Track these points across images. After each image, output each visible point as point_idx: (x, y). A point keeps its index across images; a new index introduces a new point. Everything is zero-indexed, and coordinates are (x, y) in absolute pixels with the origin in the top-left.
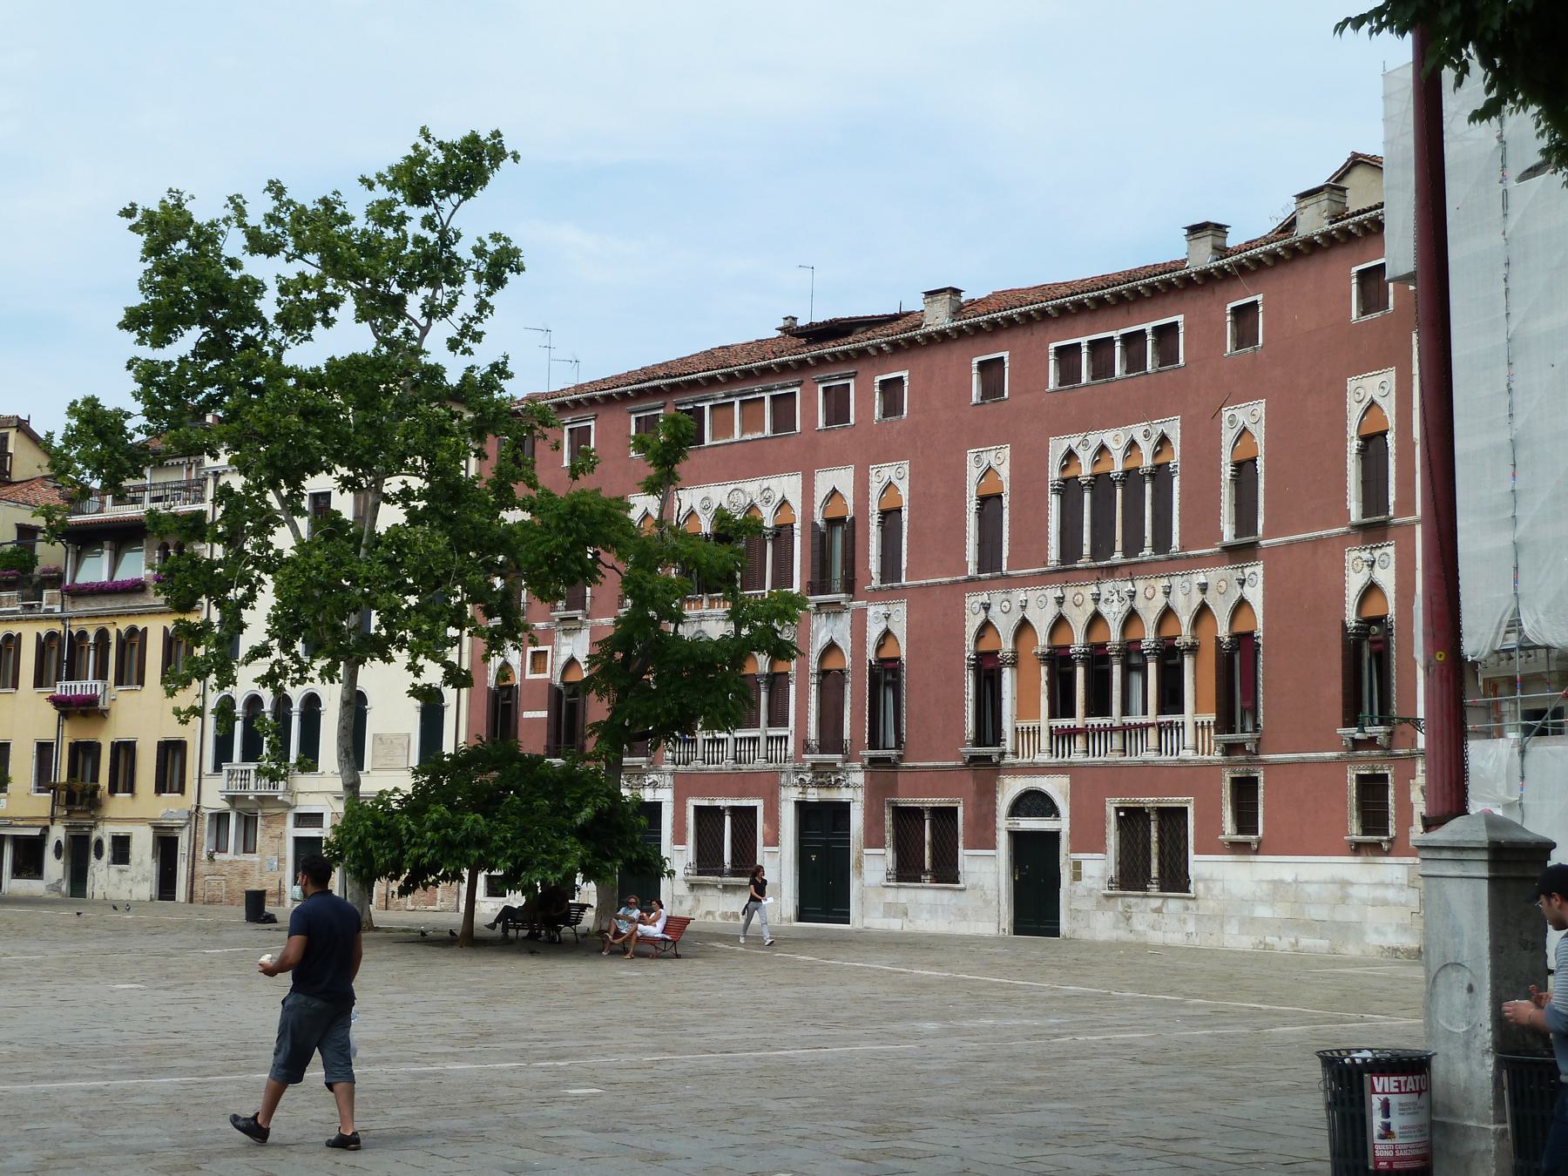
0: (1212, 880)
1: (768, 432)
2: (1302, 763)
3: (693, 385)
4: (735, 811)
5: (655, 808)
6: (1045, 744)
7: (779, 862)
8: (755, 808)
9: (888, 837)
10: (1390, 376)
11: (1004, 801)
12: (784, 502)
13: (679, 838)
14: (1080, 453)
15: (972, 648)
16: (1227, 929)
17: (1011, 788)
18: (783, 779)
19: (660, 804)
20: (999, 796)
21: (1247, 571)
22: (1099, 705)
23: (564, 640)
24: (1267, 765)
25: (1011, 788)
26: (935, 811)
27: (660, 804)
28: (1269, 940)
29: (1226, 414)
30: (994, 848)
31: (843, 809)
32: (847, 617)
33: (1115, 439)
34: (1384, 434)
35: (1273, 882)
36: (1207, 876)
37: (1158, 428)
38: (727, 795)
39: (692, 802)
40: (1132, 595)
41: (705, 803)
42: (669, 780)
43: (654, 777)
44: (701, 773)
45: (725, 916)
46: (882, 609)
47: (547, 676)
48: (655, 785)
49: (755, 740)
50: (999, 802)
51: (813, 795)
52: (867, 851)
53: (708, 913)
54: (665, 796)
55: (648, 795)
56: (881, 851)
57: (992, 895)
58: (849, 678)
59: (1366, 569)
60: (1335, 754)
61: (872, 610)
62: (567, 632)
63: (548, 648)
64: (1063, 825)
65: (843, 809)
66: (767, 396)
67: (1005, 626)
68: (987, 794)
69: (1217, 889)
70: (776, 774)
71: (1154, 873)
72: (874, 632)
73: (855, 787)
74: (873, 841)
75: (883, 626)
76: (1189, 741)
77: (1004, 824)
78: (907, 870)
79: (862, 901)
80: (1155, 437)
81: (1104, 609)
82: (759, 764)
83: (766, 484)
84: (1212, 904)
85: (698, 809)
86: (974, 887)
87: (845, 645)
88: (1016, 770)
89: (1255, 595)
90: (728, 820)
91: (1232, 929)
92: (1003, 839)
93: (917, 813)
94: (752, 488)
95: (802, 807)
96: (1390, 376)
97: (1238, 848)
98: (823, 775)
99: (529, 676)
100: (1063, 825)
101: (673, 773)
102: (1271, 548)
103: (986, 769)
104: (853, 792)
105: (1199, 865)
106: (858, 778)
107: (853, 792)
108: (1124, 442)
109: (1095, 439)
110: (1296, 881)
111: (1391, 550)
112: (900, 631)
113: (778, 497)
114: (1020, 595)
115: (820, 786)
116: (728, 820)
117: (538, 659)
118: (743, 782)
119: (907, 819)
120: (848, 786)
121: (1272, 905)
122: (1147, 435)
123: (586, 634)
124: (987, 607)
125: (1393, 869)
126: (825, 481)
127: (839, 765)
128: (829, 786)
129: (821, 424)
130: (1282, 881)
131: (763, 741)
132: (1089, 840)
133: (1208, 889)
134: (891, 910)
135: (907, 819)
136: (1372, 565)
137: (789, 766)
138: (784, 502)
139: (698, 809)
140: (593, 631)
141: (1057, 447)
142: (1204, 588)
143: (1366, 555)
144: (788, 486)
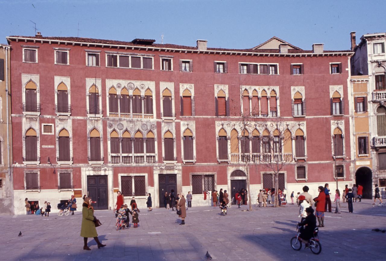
2: (320, 164)
4: (135, 177)
5: (106, 177)
6: (240, 159)
8: (144, 176)
9: (191, 182)
10: (342, 86)
12: (149, 89)
14: (249, 90)
15: (218, 135)
17: (230, 170)
18: (154, 168)
19: (107, 176)
21: (301, 123)
22: (256, 149)
23: (59, 122)
27: (107, 176)
29: (292, 88)
33: (260, 89)
34: (340, 98)
37: (272, 88)
39: (120, 175)
40: (266, 125)
43: (106, 168)
46: (186, 123)
47: (53, 134)
48: (105, 170)
49: (143, 157)
51: (165, 172)
54: (110, 174)
55: (102, 173)
56: (189, 186)
58: (175, 140)
59: (336, 124)
61: (182, 123)
65: (175, 176)
67: (229, 130)
73: (179, 170)
74: (185, 183)
75: (186, 127)
76: (283, 158)
77: (229, 178)
80: (271, 90)
81: (258, 128)
82: (145, 164)
85: (122, 177)
88: (233, 165)
89: (304, 128)
90: (133, 180)
92: (229, 182)
94: (137, 84)
95: (161, 176)
96: (342, 86)
99: (43, 133)
102: (307, 119)
104: (178, 171)
107: (178, 171)
108: (261, 90)
109: (253, 87)
111: (343, 121)
113: (147, 87)
114: (233, 123)
116: (133, 180)
117: (48, 129)
118: (143, 169)
120: (176, 170)
122: (269, 89)
123: (70, 122)
124: (222, 125)
126: (163, 85)
131: (145, 157)
132: (255, 181)
136: (337, 124)
137: (157, 164)
138: (149, 89)
139: (122, 177)
141: (244, 87)
142: (287, 125)
143: (336, 122)
144: (152, 85)
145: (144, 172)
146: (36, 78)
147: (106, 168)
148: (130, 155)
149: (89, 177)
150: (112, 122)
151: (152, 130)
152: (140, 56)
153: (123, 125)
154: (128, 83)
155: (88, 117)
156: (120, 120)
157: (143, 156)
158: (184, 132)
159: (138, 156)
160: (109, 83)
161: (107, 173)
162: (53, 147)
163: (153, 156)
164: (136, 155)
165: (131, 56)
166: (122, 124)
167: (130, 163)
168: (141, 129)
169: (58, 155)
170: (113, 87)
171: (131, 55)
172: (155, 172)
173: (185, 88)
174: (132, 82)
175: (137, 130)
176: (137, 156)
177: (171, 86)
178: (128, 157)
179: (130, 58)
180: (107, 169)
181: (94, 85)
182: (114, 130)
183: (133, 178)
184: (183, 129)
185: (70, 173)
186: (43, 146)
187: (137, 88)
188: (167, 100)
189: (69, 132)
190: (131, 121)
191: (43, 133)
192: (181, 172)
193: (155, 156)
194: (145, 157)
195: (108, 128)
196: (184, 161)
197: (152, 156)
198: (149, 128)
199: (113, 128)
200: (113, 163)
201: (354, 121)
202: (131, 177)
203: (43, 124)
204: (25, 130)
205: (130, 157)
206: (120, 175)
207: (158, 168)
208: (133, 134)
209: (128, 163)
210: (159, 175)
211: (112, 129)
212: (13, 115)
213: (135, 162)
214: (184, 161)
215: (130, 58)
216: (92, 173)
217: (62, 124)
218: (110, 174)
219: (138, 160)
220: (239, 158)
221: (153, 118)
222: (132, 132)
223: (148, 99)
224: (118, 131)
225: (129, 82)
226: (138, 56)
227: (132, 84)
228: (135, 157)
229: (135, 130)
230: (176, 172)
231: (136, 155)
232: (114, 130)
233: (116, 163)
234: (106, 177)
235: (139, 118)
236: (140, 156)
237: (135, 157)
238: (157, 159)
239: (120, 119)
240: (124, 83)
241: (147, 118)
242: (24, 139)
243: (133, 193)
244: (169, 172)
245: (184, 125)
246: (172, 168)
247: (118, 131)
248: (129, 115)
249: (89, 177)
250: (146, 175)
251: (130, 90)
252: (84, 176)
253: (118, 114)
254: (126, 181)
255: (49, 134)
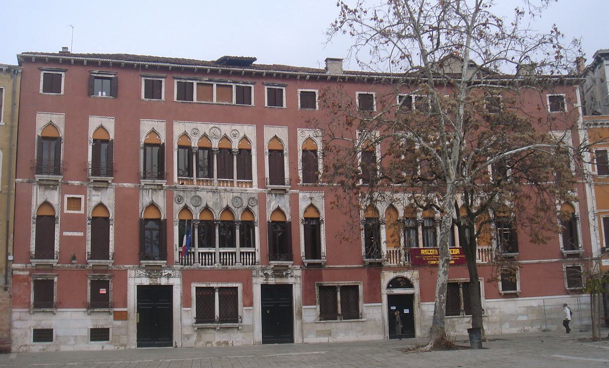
0: (494, 308)
1: (234, 102)
2: (540, 263)
3: (191, 71)
4: (220, 289)
5: (170, 288)
7: (252, 315)
11: (385, 282)
13: (186, 303)
16: (503, 327)
17: (387, 277)
18: (254, 273)
19: (172, 286)
20: (382, 280)
23: (94, 192)
24: (521, 266)
25: (387, 277)
26: (344, 288)
27: (172, 286)
28: (526, 328)
30: (381, 302)
31: (290, 287)
32: (287, 197)
35: (527, 307)
36: (492, 307)
38: (218, 281)
39: (194, 286)
41: (204, 285)
42: (178, 273)
43: (170, 272)
44: (200, 270)
45: (219, 343)
46: (308, 195)
47: (82, 212)
48: (169, 276)
50: (382, 282)
51: (272, 281)
52: (304, 307)
53: (208, 343)
54: (176, 282)
55: (163, 281)
56: (315, 307)
57: (380, 323)
60: (557, 260)
61: (301, 195)
62: (96, 188)
63: (82, 197)
64: (416, 290)
65: (290, 287)
66: (234, 86)
67: (382, 208)
68: (375, 280)
69: (497, 311)
70: (251, 270)
71: (462, 308)
72: (303, 205)
75: (309, 202)
77: (385, 292)
78: (328, 314)
79: (302, 331)
82: (238, 266)
83: (234, 127)
84: (495, 318)
86: (370, 320)
87: (287, 210)
88: (390, 269)
90: (217, 294)
91: (507, 325)
92: (385, 298)
93: (333, 289)
94: (226, 129)
95: (264, 287)
97: (506, 296)
98: (279, 272)
99: (66, 211)
100: (416, 290)
101: (181, 270)
103: (376, 268)
104: (295, 279)
105: (486, 303)
106: (298, 273)
110: (539, 306)
112: (320, 204)
113: (242, 135)
115: (276, 276)
116: (217, 294)
117: (75, 203)
119: (327, 293)
120: (292, 277)
121: (527, 315)
125: (586, 298)
126: (269, 132)
127: (290, 266)
128: (282, 277)
129: (266, 105)
130: (531, 307)
131: (238, 254)
132: (426, 296)
133: (493, 312)
134: (319, 333)
135: (327, 293)
138: (245, 138)
140: (118, 191)
144: (249, 131)
145: (237, 282)
146: (59, 119)
147: (170, 272)
148: (212, 250)
149: (141, 289)
150: (181, 194)
151: (250, 207)
152: (231, 84)
153: (201, 198)
154: (211, 127)
155: (143, 184)
156: (196, 189)
157: (235, 253)
158: (305, 211)
159: (226, 253)
160: (179, 128)
161: (171, 281)
162: (81, 234)
163: (252, 253)
164: (222, 250)
165: (217, 83)
166: (198, 196)
167: (212, 265)
168: (230, 205)
169: (88, 249)
170: (185, 134)
171: (215, 81)
172: (254, 280)
173: (307, 136)
174: (217, 126)
175: (224, 207)
176: (223, 253)
177: (282, 133)
178: (208, 253)
179: (215, 86)
180: (172, 275)
181: (153, 131)
182: (186, 208)
183: (217, 290)
184: (303, 205)
185: (109, 281)
186: (66, 234)
187: (226, 137)
188: (276, 156)
189: (109, 209)
190: (214, 192)
191: (66, 211)
192: (299, 281)
193: (255, 253)
194: (238, 254)
195: (175, 204)
196: (306, 261)
197: (249, 253)
198: (245, 204)
199: (183, 204)
200: (182, 264)
201: (593, 190)
202: (212, 289)
203: (66, 196)
204: (37, 205)
205: (211, 253)
206: (194, 286)
207: (261, 274)
208: (217, 214)
209: (209, 265)
210: (262, 286)
211: (182, 206)
212: (17, 180)
213: (220, 262)
214: (306, 261)
215: (215, 86)
216: (146, 281)
217: (98, 196)
218: (176, 282)
219: (226, 259)
220: (400, 256)
221: (251, 186)
222: (216, 211)
223: (245, 154)
224: (193, 208)
225: (212, 126)
226: (228, 84)
227: (217, 130)
228: (220, 253)
229: (221, 207)
230: (290, 281)
231: (222, 250)
232: (186, 208)
233: (188, 265)
234: (170, 288)
235: (227, 186)
236: (229, 253)
237: (220, 253)
238: (258, 258)
239: (195, 188)
240: (204, 128)
241: (242, 186)
242: (35, 221)
243: (216, 318)
244: (279, 281)
245: (304, 198)
246: (284, 273)
247: (193, 208)
248: (211, 181)
249: (141, 289)
250: (239, 286)
251: (214, 140)
252: (133, 287)
253: (192, 180)
254: (204, 297)
255: (76, 212)
